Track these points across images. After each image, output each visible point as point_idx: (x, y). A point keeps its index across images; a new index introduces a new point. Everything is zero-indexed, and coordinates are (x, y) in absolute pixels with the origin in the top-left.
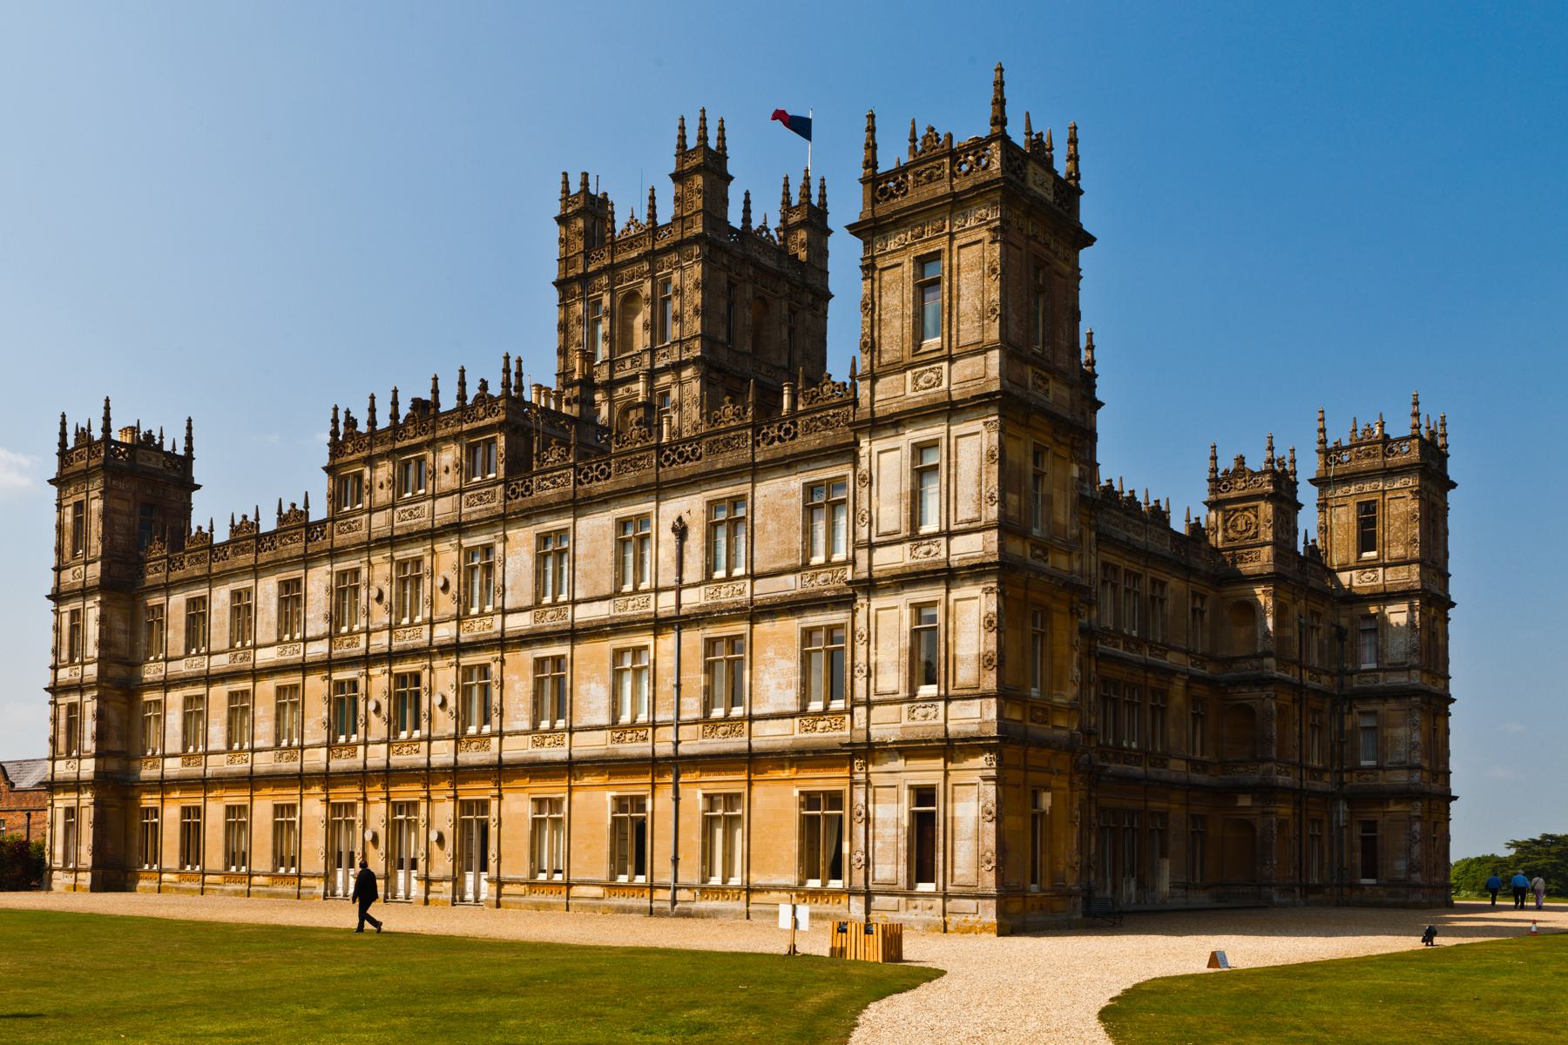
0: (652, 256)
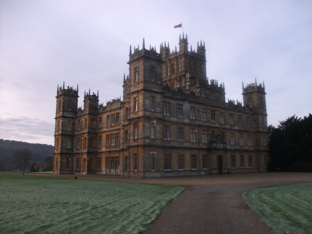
0: (176, 57)
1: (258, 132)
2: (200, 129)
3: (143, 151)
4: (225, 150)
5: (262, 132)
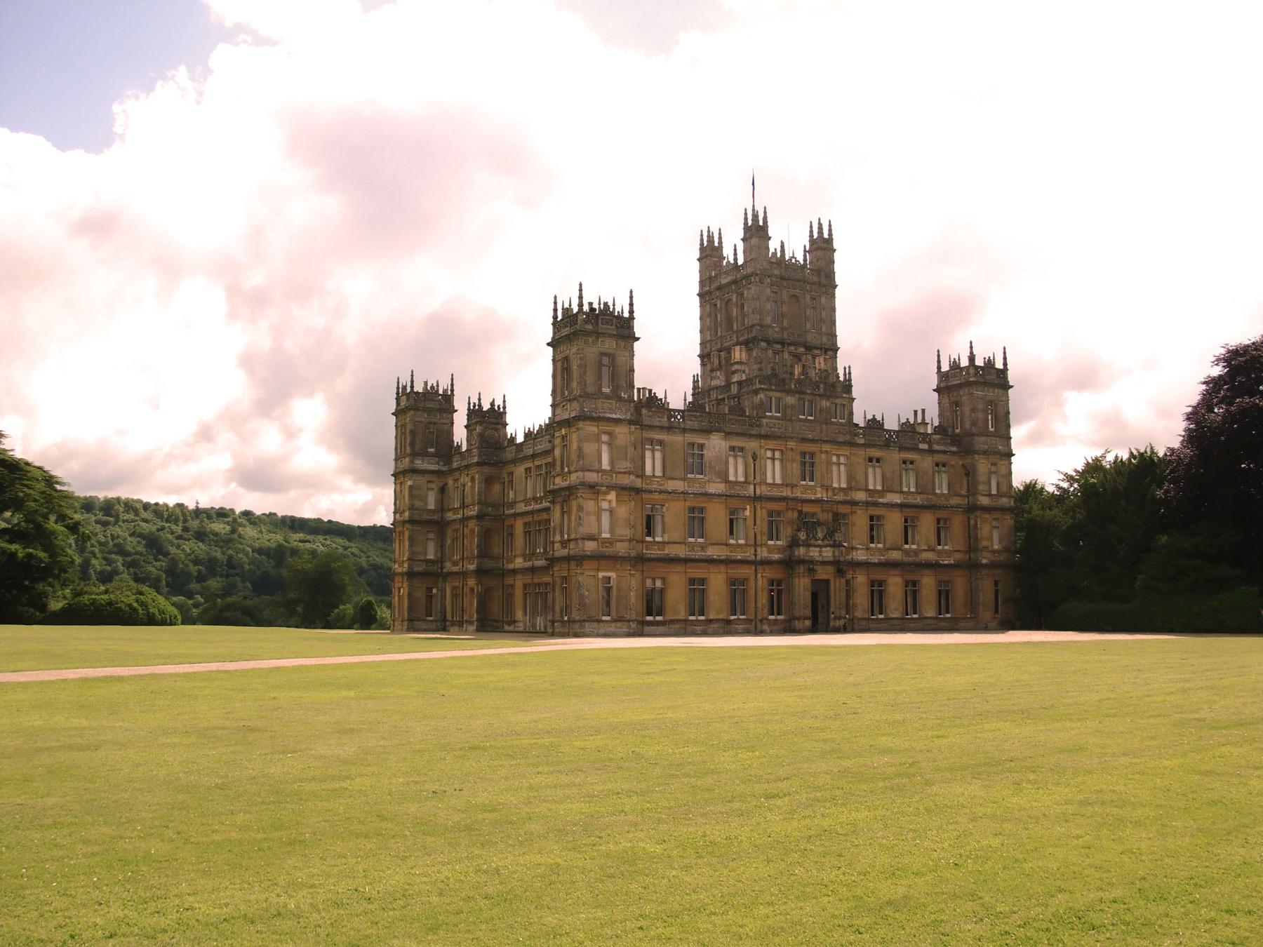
4: (841, 567)
5: (988, 509)
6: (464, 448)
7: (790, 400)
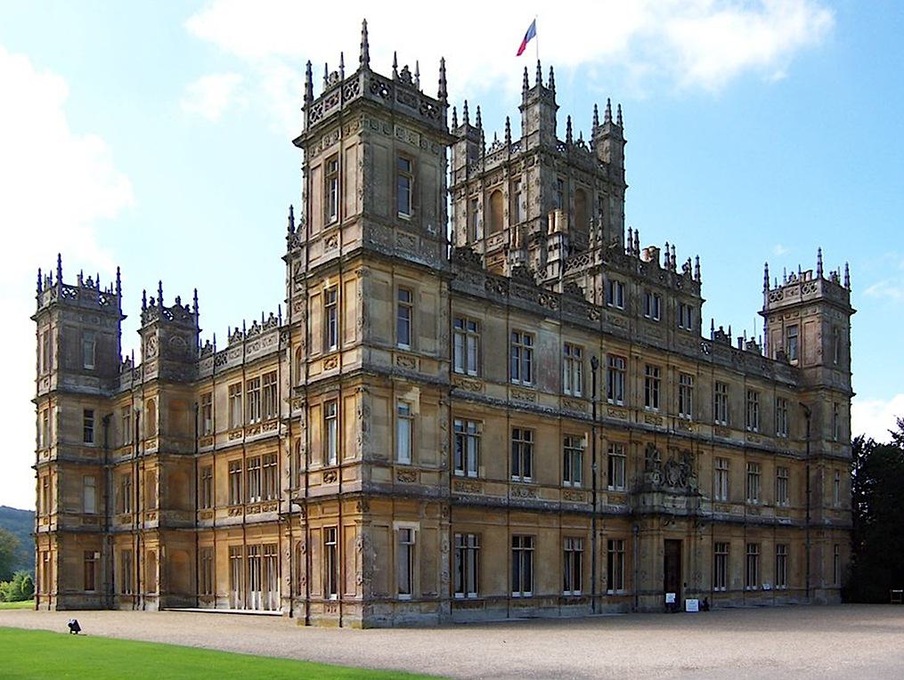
1: (814, 458)
2: (598, 436)
3: (361, 518)
5: (831, 458)
6: (137, 362)
7: (636, 289)
